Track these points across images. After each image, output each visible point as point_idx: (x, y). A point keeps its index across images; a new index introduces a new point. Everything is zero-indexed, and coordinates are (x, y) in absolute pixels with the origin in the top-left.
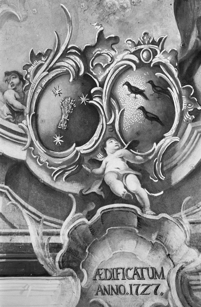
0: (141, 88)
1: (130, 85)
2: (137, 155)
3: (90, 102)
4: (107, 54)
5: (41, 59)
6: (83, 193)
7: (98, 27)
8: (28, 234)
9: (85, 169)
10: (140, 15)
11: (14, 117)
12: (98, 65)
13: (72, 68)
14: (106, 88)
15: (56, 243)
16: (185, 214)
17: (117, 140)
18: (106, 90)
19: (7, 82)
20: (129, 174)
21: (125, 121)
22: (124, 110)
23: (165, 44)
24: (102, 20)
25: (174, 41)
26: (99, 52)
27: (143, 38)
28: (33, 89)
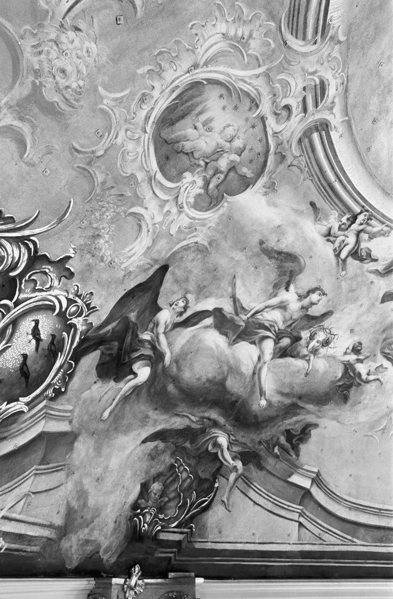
0: (43, 336)
4: (52, 279)
7: (72, 251)
10: (104, 276)
12: (35, 281)
13: (10, 260)
22: (10, 346)
23: (93, 314)
26: (47, 271)
27: (87, 294)
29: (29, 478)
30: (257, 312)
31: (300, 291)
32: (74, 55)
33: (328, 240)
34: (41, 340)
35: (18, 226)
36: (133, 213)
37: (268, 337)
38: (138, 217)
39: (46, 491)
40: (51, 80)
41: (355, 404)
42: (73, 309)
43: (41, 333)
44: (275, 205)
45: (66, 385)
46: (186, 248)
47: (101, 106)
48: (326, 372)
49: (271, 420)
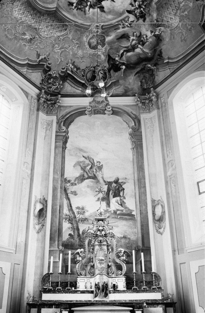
0: (102, 73)
30: (131, 45)
31: (132, 36)
33: (124, 28)
37: (138, 45)
41: (163, 39)
42: (103, 68)
44: (111, 35)
46: (108, 51)
48: (153, 40)
49: (154, 55)
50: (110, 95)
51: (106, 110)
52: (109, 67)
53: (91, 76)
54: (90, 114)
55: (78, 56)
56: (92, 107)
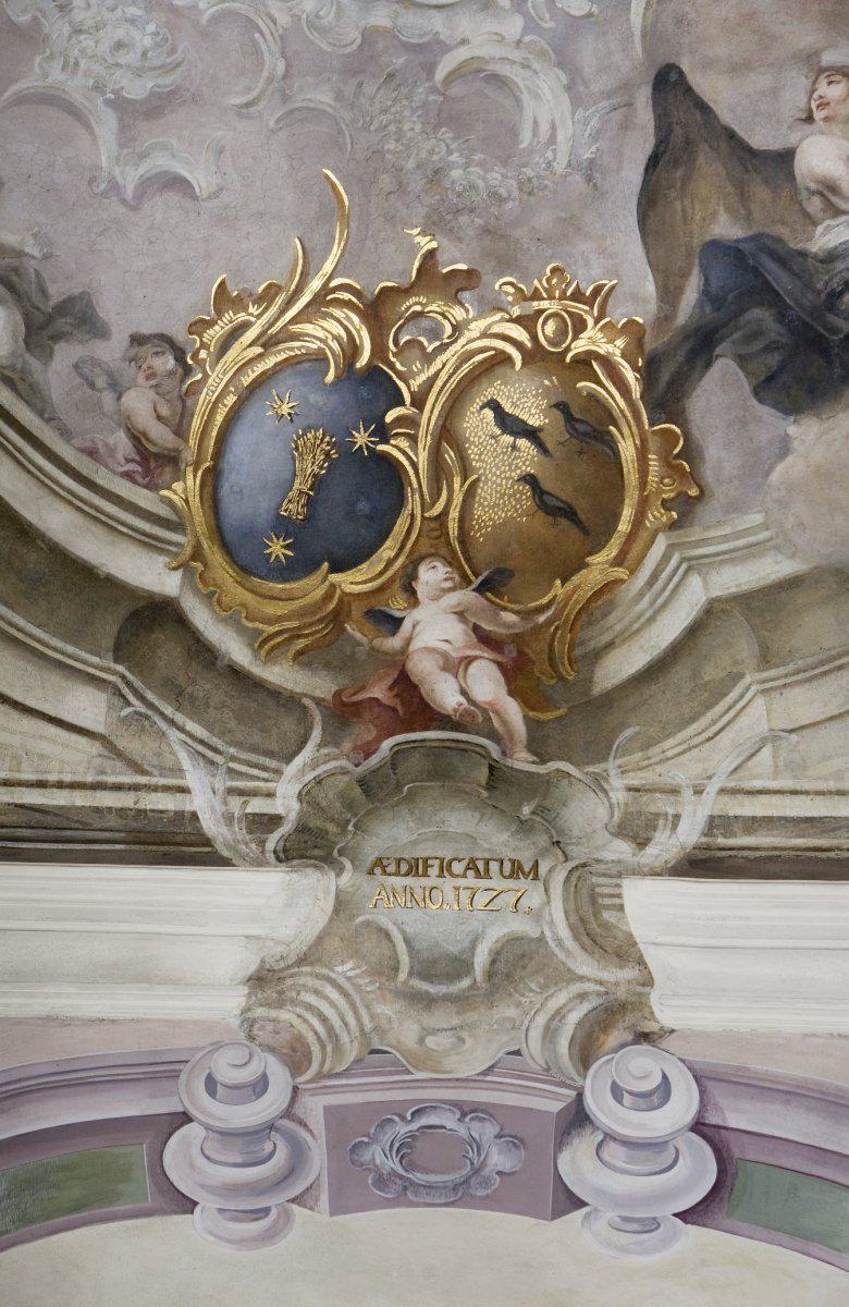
0: (534, 421)
1: (503, 410)
2: (505, 609)
3: (381, 447)
4: (443, 314)
5: (245, 309)
6: (344, 699)
7: (422, 240)
8: (184, 790)
9: (353, 637)
11: (147, 472)
13: (335, 345)
14: (432, 412)
15: (265, 815)
16: (620, 767)
17: (450, 564)
18: (430, 417)
19: (133, 364)
20: (476, 658)
21: (478, 512)
22: (477, 480)
23: (610, 302)
24: (434, 223)
25: (634, 297)
26: (418, 308)
27: (548, 280)
28: (213, 392)
29: (747, 704)
32: (107, 15)
34: (540, 429)
35: (293, 287)
36: (454, 71)
38: (471, 71)
39: (832, 718)
40: (119, 72)
43: (524, 416)
45: (694, 477)
47: (206, 17)
50: (668, 845)
51: (577, 1118)
52: (663, 319)
53: (310, 466)
54: (255, 1189)
55: (75, 88)
56: (296, 1057)
